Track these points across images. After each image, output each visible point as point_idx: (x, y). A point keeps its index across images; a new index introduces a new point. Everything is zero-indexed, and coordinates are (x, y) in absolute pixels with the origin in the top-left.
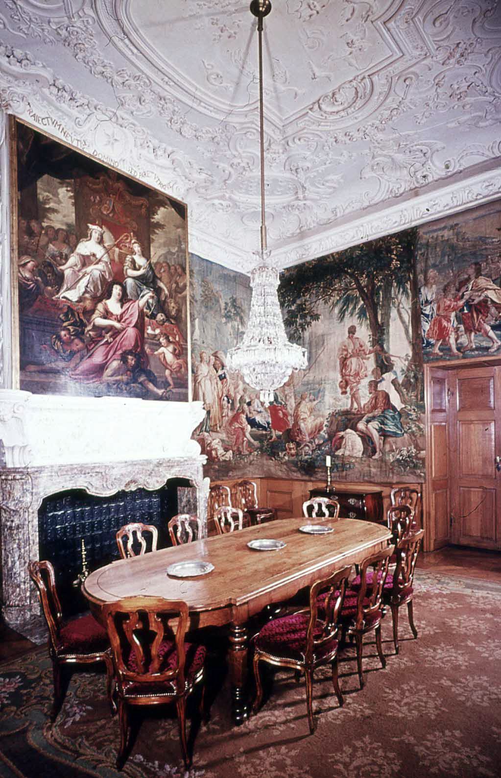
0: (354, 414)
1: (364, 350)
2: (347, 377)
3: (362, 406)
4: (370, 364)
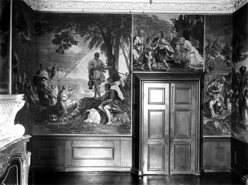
0: (96, 100)
1: (103, 67)
2: (93, 80)
3: (101, 96)
4: (107, 75)
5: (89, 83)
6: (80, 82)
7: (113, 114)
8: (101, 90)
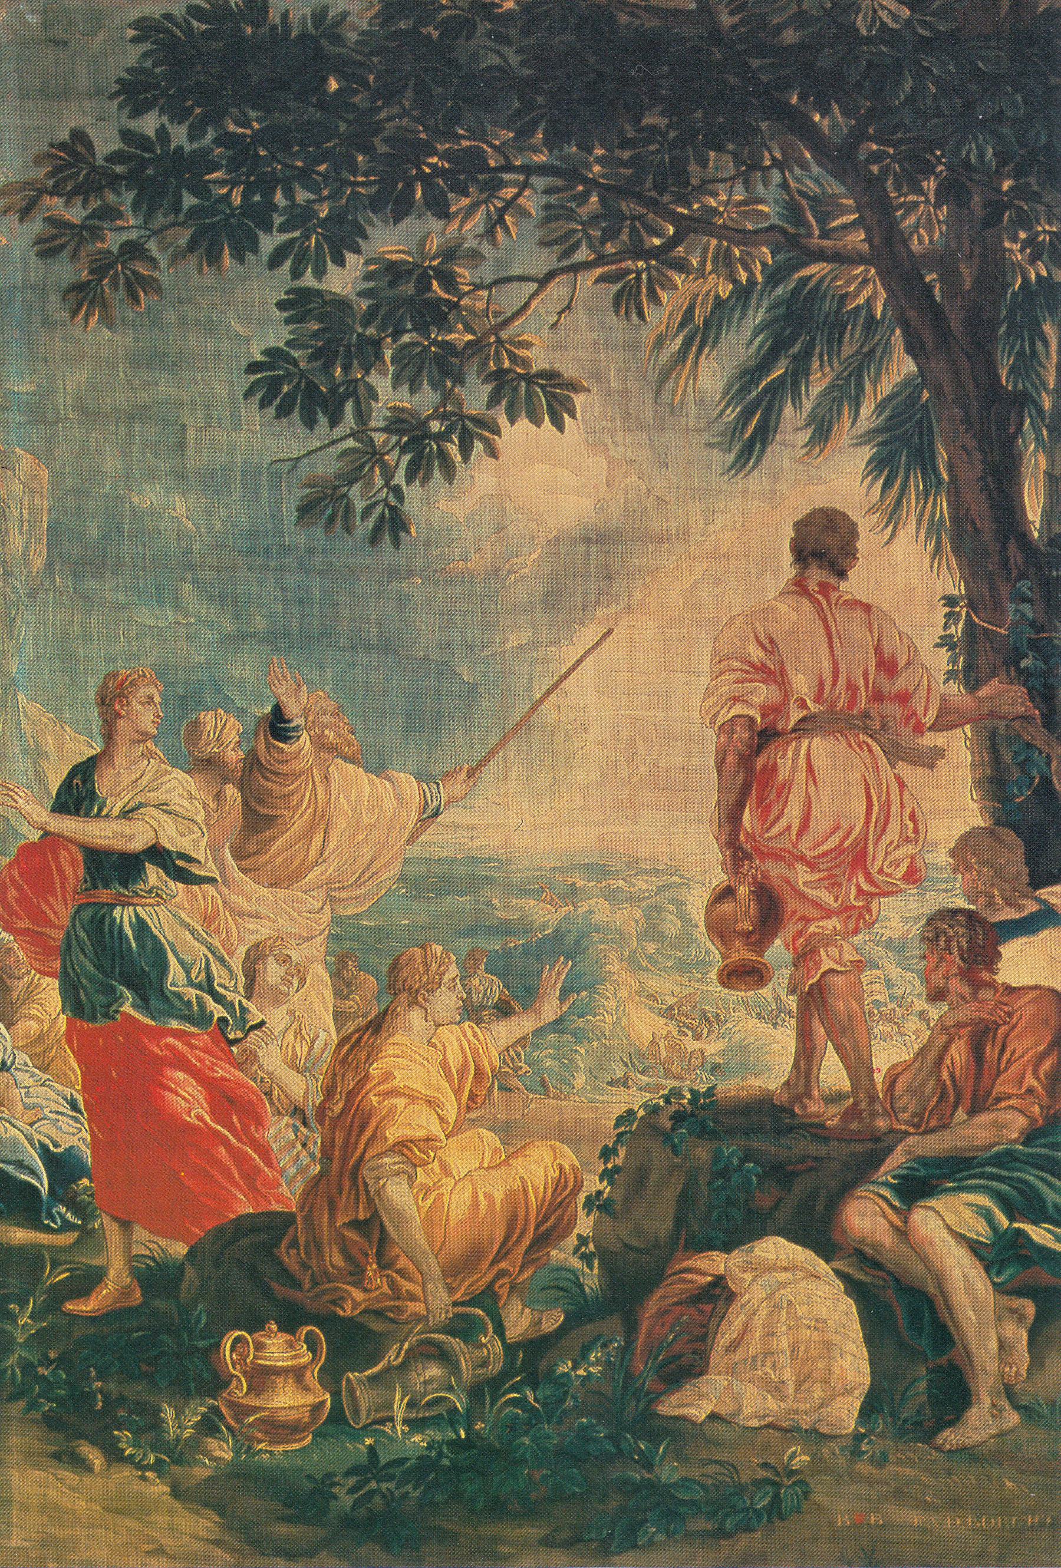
0: (817, 1131)
1: (904, 698)
5: (727, 907)
6: (612, 896)
7: (1030, 1308)
8: (875, 992)
